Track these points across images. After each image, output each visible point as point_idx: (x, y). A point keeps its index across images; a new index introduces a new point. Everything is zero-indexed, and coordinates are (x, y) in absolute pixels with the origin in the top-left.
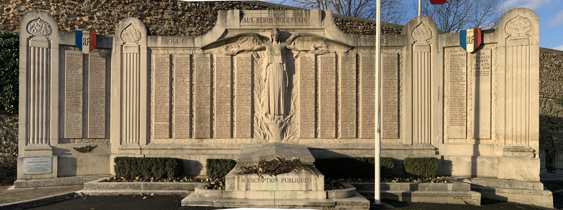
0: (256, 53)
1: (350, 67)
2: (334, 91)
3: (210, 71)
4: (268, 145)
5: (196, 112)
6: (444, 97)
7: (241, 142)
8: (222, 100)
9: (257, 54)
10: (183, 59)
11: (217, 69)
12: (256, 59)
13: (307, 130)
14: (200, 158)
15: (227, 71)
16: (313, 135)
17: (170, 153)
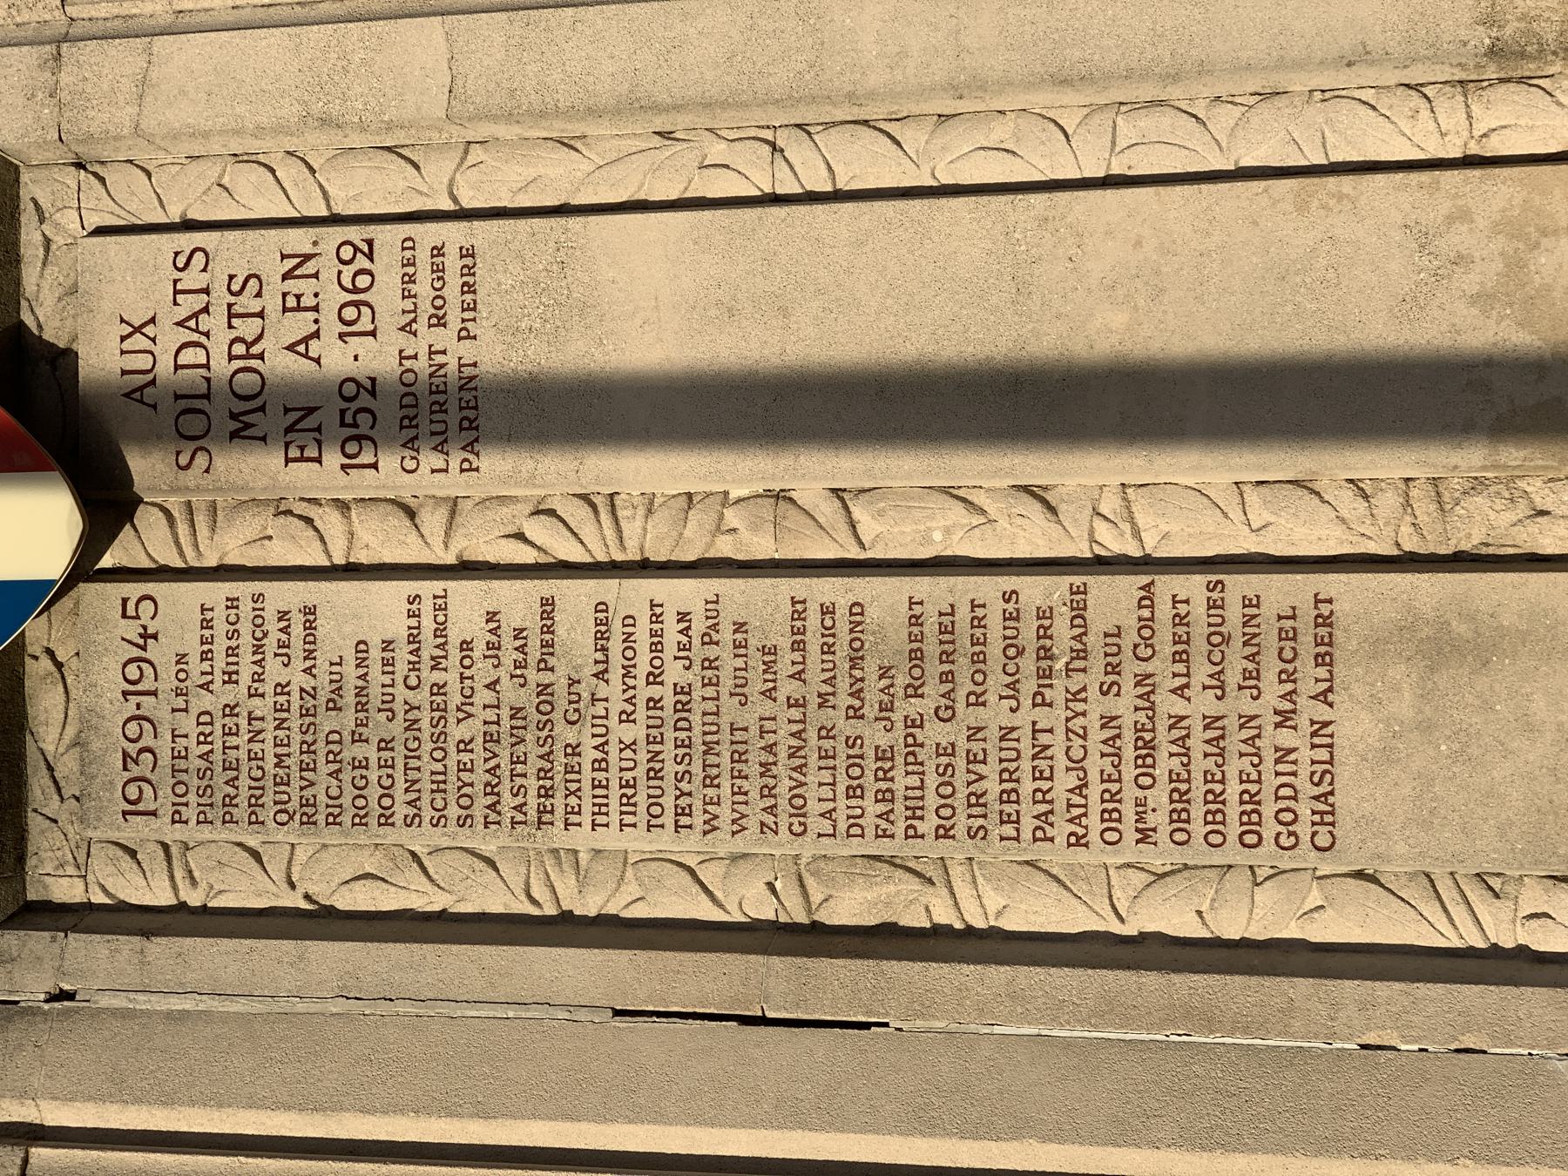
6: (816, 928)
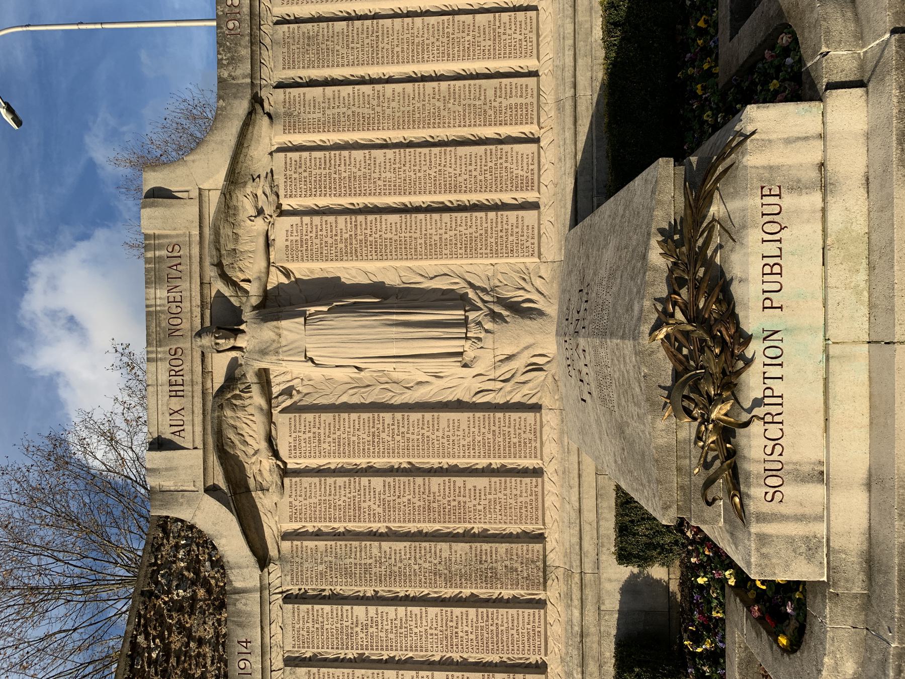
0: (277, 397)
1: (314, 107)
2: (390, 153)
3: (333, 543)
4: (569, 362)
5: (461, 587)
7: (554, 444)
8: (422, 503)
9: (280, 395)
10: (297, 626)
11: (325, 519)
12: (296, 397)
13: (512, 235)
14: (610, 580)
15: (333, 489)
16: (530, 216)
17: (596, 674)
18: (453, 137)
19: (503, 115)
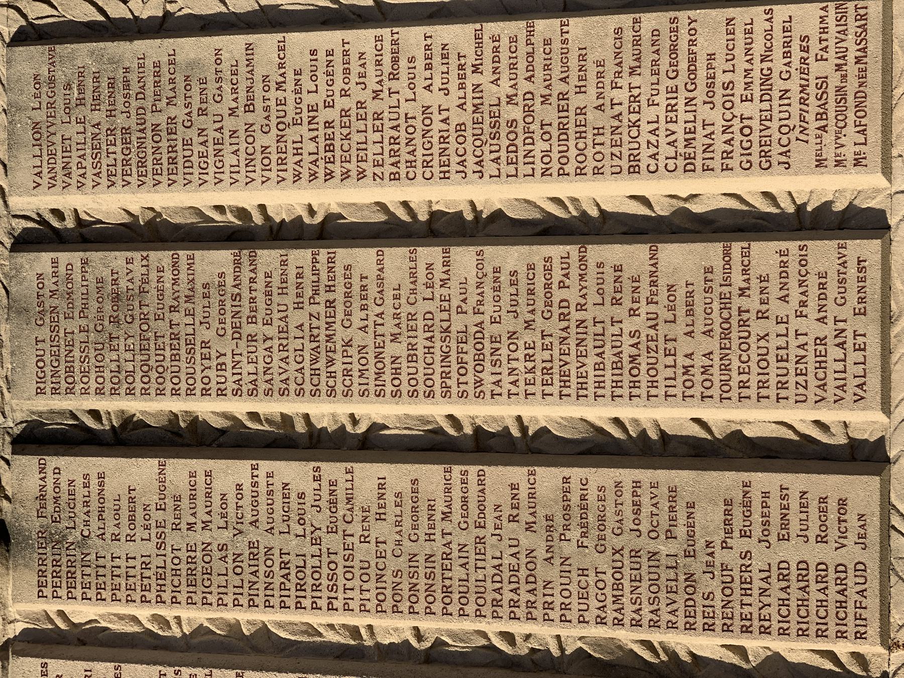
1: (132, 519)
18: (579, 644)
19: (754, 599)
